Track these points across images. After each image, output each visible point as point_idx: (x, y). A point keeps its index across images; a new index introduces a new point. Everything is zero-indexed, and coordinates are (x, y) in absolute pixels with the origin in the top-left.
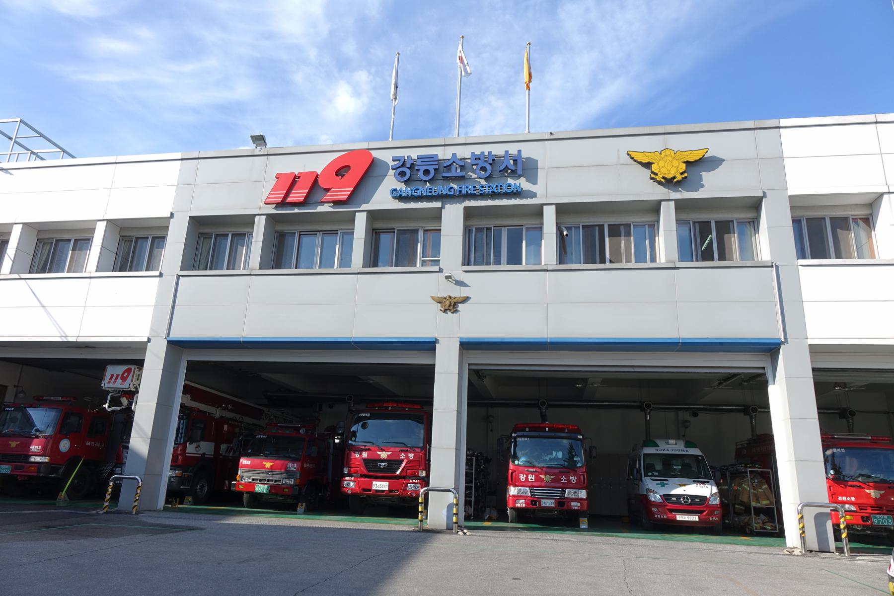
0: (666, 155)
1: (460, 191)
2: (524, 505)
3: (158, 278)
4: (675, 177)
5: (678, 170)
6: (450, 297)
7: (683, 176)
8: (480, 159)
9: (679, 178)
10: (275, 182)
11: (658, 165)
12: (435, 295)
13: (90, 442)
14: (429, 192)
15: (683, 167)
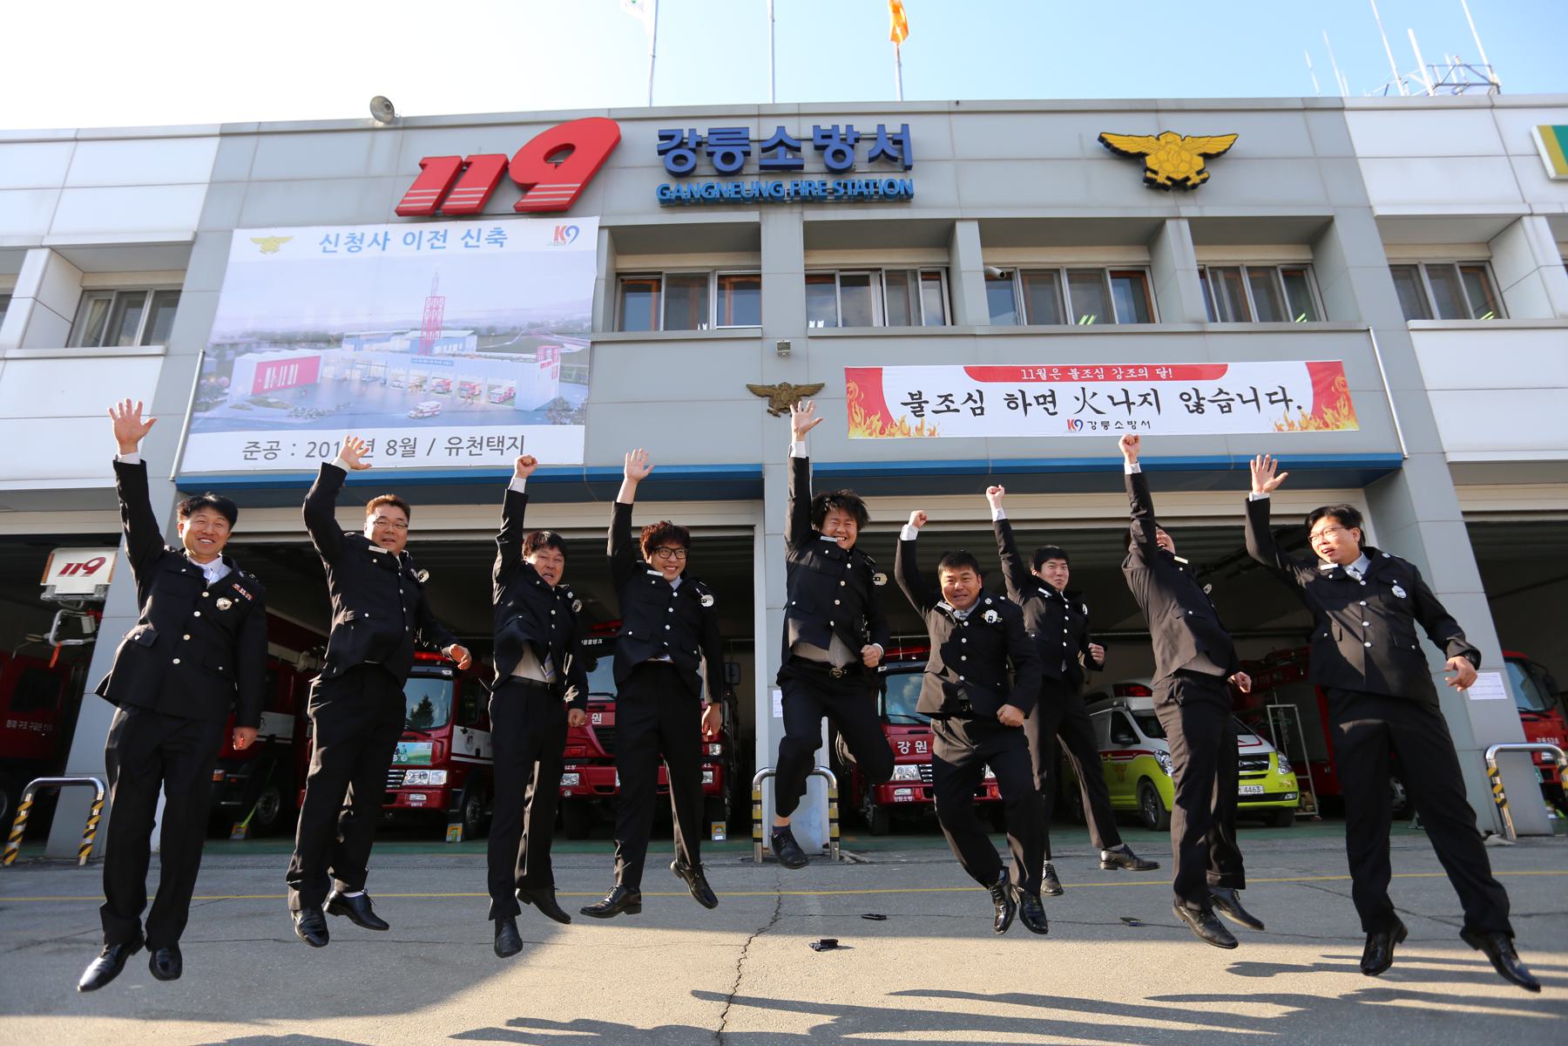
0: (1167, 143)
1: (797, 193)
2: (910, 798)
3: (162, 358)
4: (1187, 179)
5: (1191, 167)
6: (789, 386)
7: (1202, 176)
8: (830, 137)
9: (1195, 179)
10: (416, 178)
11: (1157, 158)
12: (757, 382)
13: (15, 722)
14: (736, 193)
15: (1199, 163)
